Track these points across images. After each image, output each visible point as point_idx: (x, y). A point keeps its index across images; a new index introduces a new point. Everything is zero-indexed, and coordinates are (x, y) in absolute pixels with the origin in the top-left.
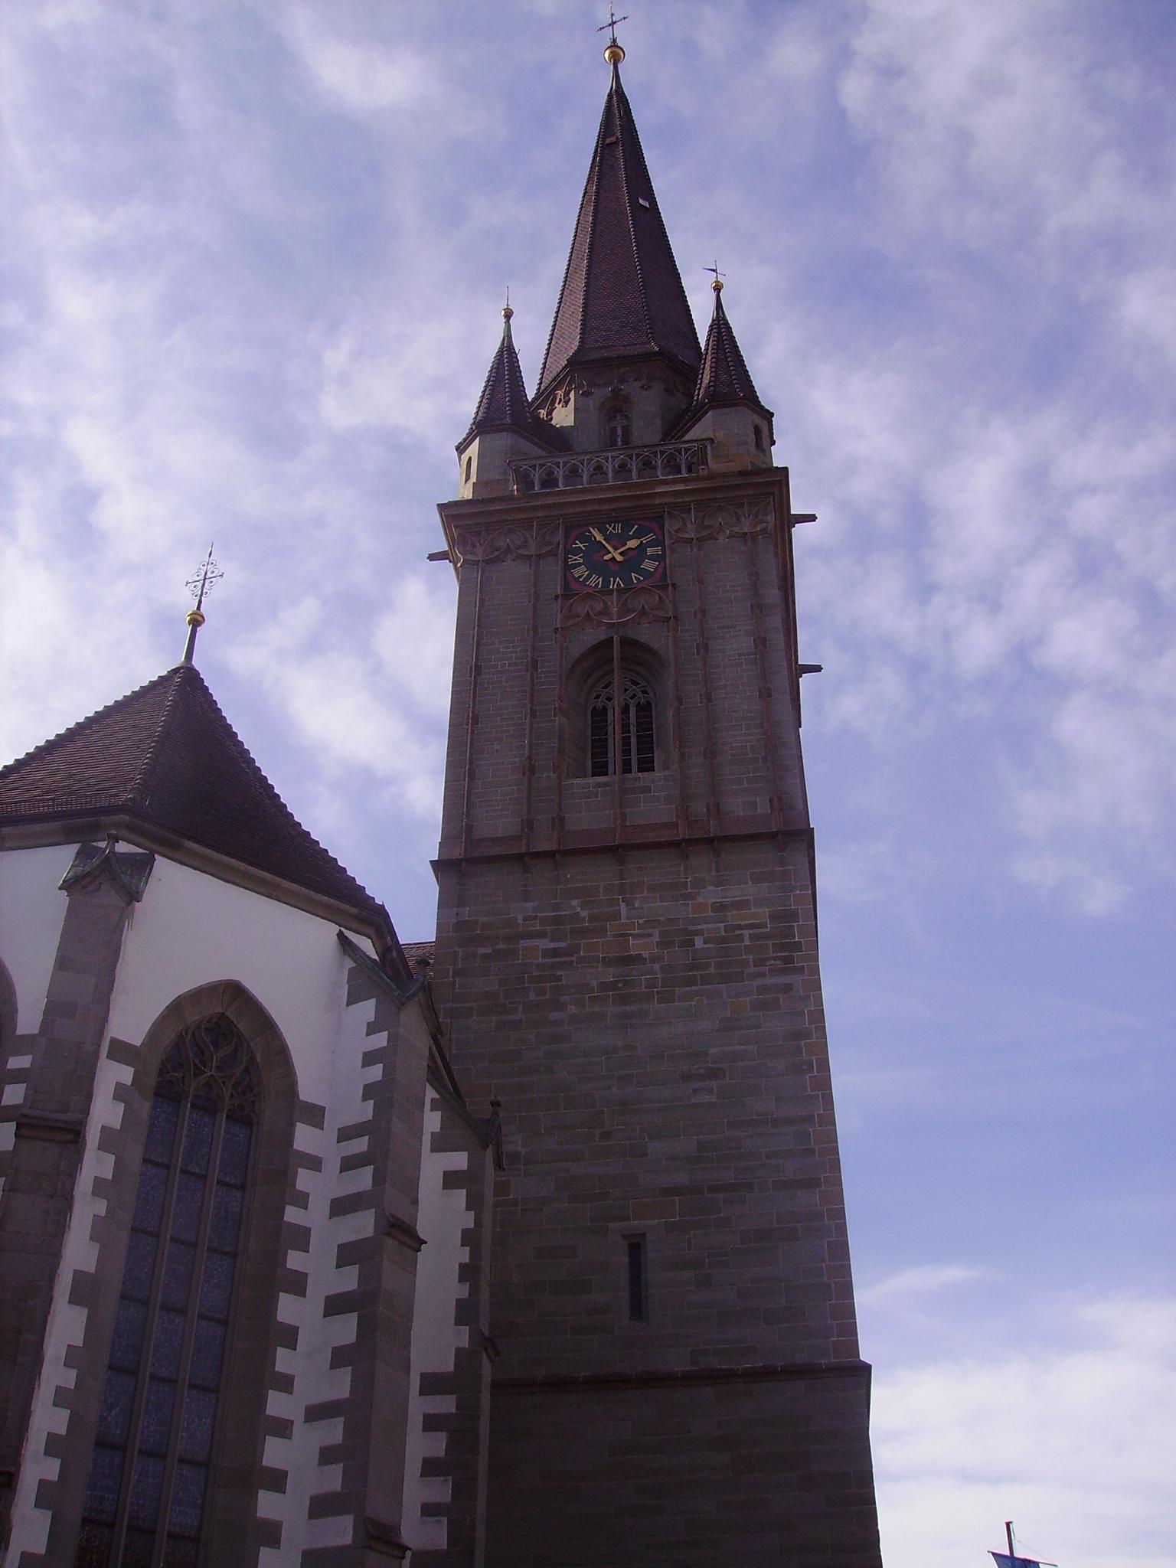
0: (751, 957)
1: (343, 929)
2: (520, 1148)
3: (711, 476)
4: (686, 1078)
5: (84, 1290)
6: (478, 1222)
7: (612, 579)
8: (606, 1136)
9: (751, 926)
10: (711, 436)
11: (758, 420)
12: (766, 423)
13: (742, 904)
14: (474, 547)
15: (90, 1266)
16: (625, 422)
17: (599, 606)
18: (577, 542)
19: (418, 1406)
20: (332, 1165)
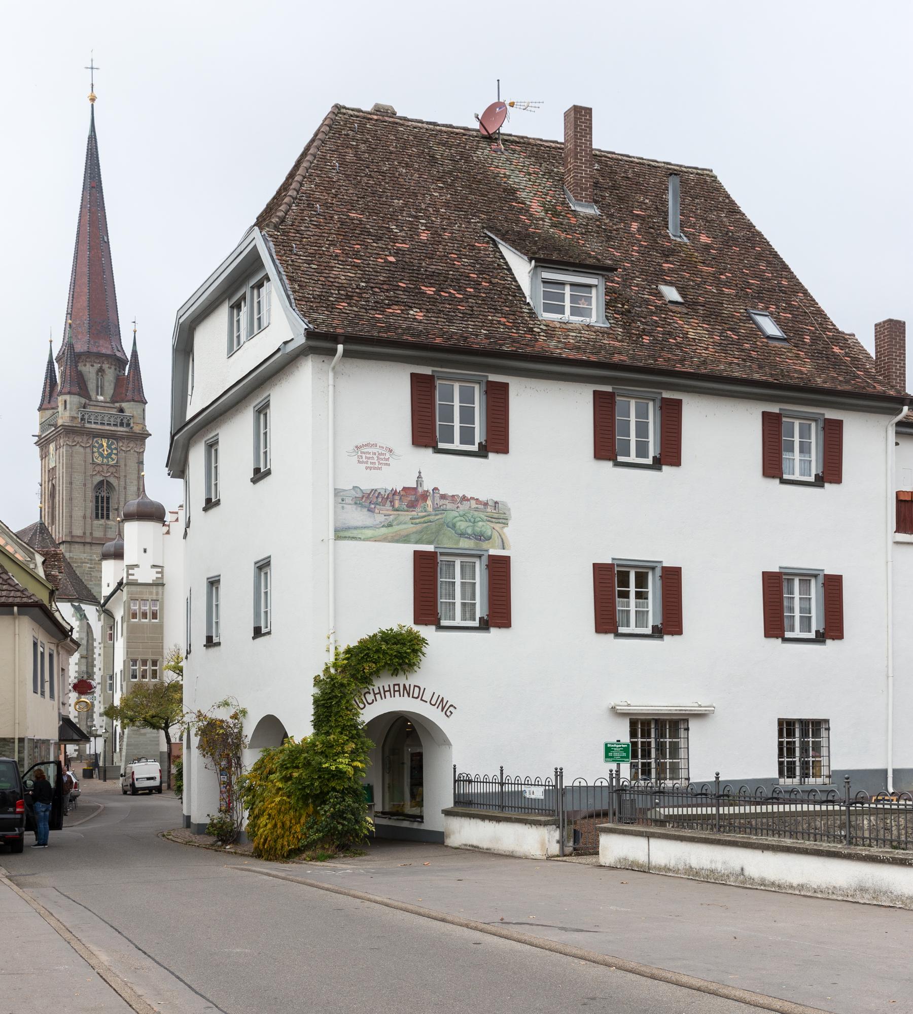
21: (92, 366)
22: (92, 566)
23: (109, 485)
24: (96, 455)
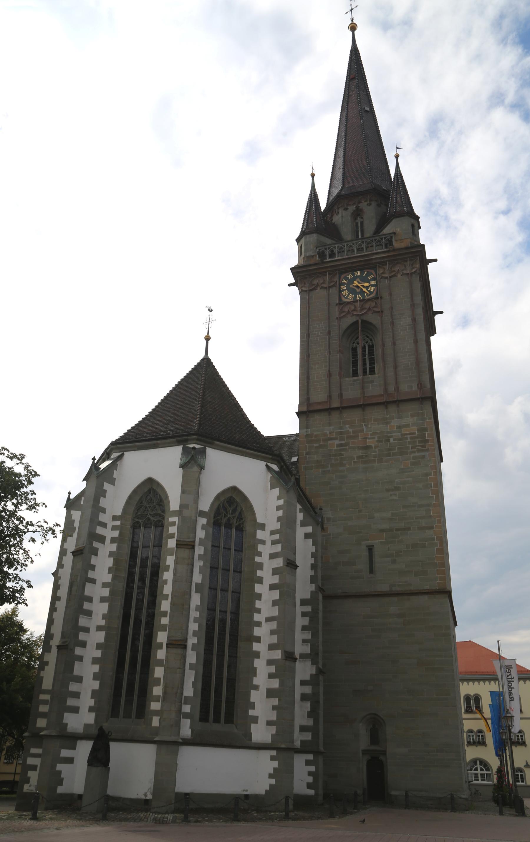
0: (410, 446)
1: (267, 463)
2: (331, 516)
3: (394, 250)
4: (388, 490)
5: (199, 588)
6: (316, 550)
7: (357, 295)
8: (360, 511)
9: (410, 434)
10: (395, 231)
11: (413, 221)
12: (417, 221)
13: (407, 426)
14: (305, 284)
15: (200, 581)
16: (361, 220)
17: (353, 308)
18: (344, 280)
19: (299, 609)
20: (268, 543)
21: (346, 209)
22: (343, 442)
23: (367, 326)
24: (345, 293)
